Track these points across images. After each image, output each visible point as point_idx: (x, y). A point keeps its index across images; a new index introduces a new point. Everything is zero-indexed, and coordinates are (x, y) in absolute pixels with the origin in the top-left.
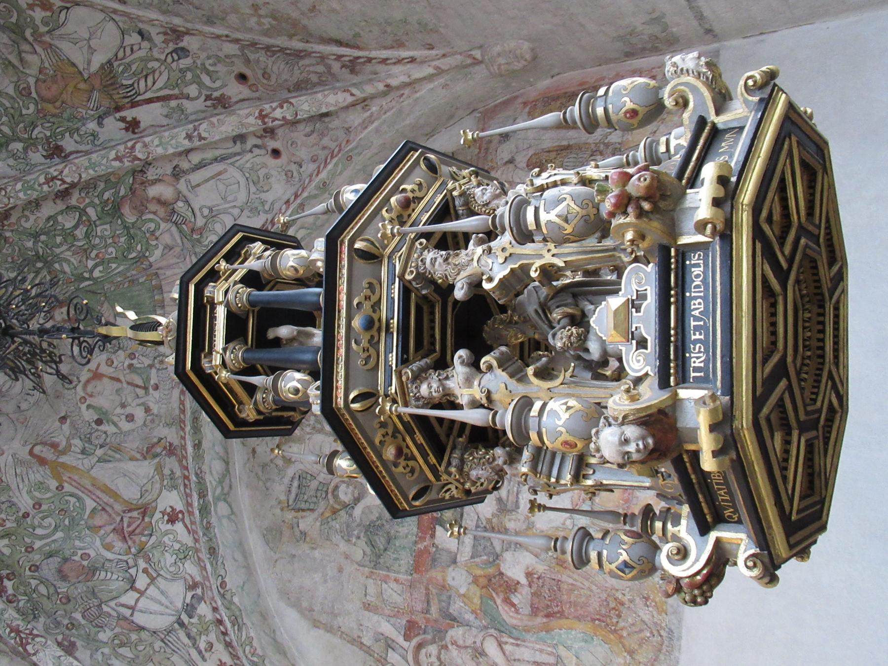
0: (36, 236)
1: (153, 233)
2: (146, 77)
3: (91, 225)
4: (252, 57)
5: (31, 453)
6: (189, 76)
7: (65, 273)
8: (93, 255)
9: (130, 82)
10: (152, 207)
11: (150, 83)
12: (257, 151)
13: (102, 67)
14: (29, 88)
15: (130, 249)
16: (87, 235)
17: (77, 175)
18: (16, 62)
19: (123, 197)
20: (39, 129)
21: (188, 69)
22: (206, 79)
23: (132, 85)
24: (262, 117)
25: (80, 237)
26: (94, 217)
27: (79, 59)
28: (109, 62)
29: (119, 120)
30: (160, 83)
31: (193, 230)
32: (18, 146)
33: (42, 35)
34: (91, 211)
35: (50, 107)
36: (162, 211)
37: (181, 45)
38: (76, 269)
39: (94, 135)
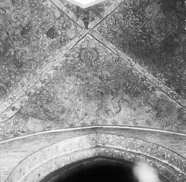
2: (16, 123)
3: (12, 79)
5: (6, 11)
6: (6, 128)
7: (12, 65)
8: (7, 72)
9: (19, 120)
11: (15, 122)
13: (28, 120)
14: (41, 108)
16: (11, 76)
17: (23, 89)
18: (47, 113)
19: (7, 89)
20: (35, 99)
23: (19, 119)
25: (13, 75)
26: (11, 81)
27: (35, 120)
29: (17, 109)
30: (12, 122)
32: (38, 92)
33: (45, 121)
35: (35, 105)
37: (13, 135)
38: (10, 67)
39: (21, 102)
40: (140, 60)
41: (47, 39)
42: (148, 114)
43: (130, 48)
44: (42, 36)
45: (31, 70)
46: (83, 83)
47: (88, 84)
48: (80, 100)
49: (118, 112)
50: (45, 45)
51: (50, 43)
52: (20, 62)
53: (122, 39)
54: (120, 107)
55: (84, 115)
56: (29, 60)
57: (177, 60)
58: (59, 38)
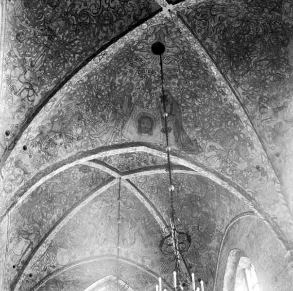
0: (54, 207)
1: (29, 225)
3: (43, 217)
4: (33, 283)
6: (40, 265)
10: (32, 232)
12: (18, 263)
15: (32, 217)
16: (43, 214)
21: (41, 267)
22: (37, 268)
24: (25, 274)
27: (62, 250)
28: (56, 255)
31: (21, 233)
34: (44, 220)
36: (30, 232)
40: (163, 208)
41: (79, 173)
42: (155, 255)
43: (157, 192)
44: (74, 170)
45: (61, 205)
46: (108, 205)
47: (111, 206)
48: (102, 224)
49: (132, 244)
50: (77, 178)
51: (82, 176)
52: (51, 195)
53: (152, 183)
54: (135, 239)
55: (103, 240)
56: (60, 193)
57: (192, 222)
58: (90, 173)
